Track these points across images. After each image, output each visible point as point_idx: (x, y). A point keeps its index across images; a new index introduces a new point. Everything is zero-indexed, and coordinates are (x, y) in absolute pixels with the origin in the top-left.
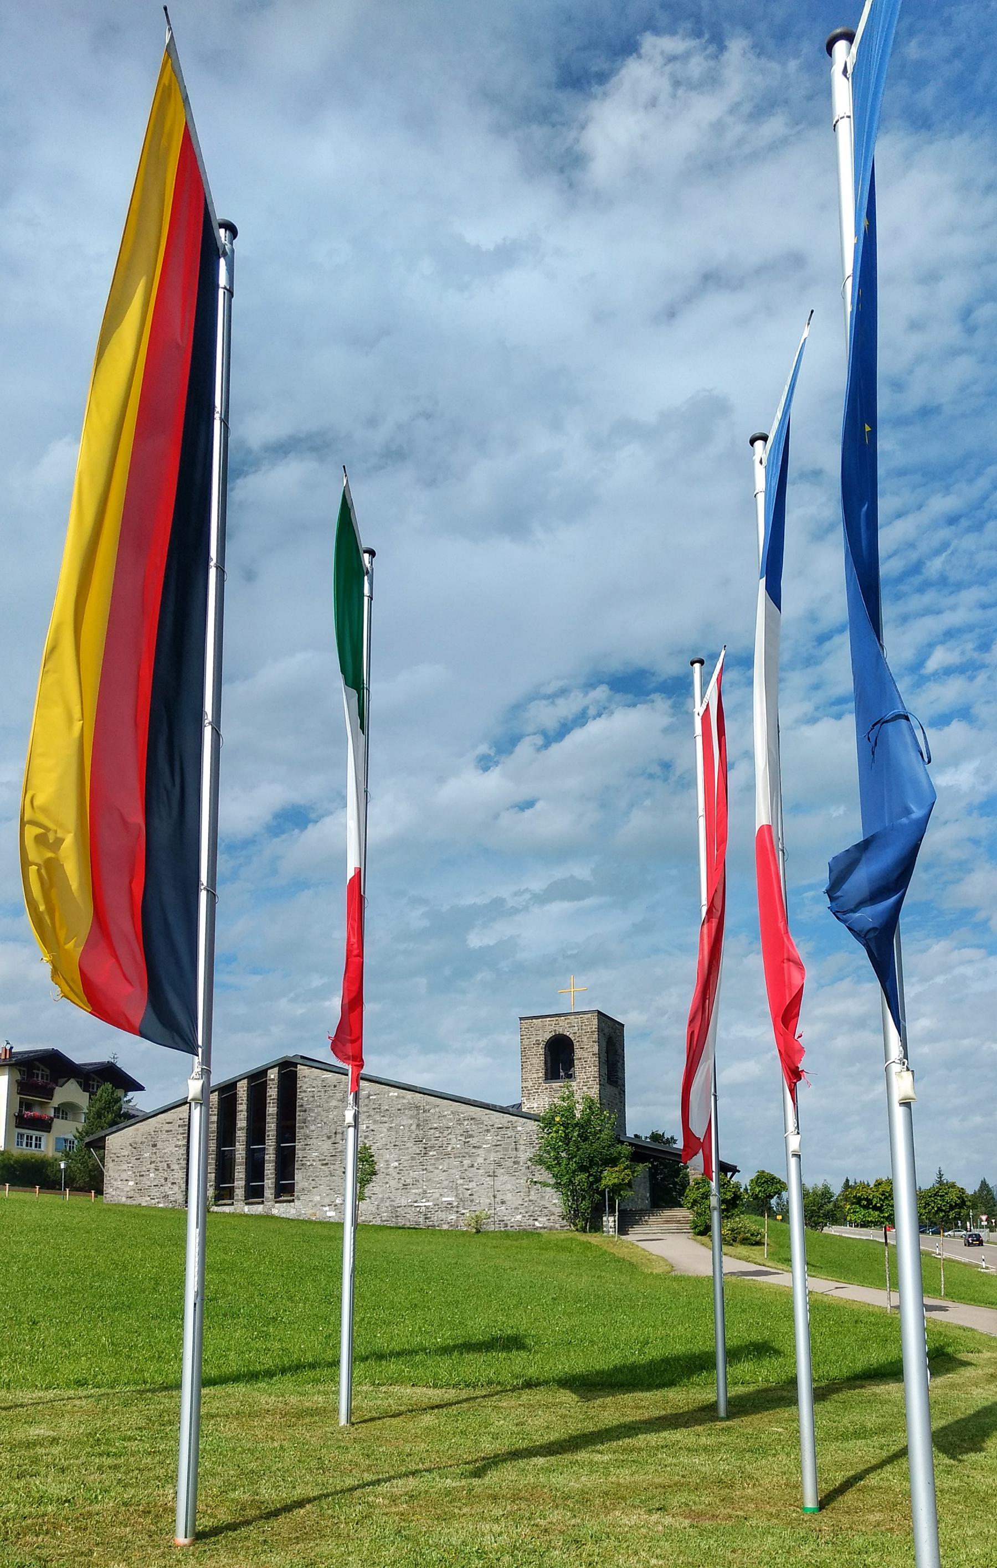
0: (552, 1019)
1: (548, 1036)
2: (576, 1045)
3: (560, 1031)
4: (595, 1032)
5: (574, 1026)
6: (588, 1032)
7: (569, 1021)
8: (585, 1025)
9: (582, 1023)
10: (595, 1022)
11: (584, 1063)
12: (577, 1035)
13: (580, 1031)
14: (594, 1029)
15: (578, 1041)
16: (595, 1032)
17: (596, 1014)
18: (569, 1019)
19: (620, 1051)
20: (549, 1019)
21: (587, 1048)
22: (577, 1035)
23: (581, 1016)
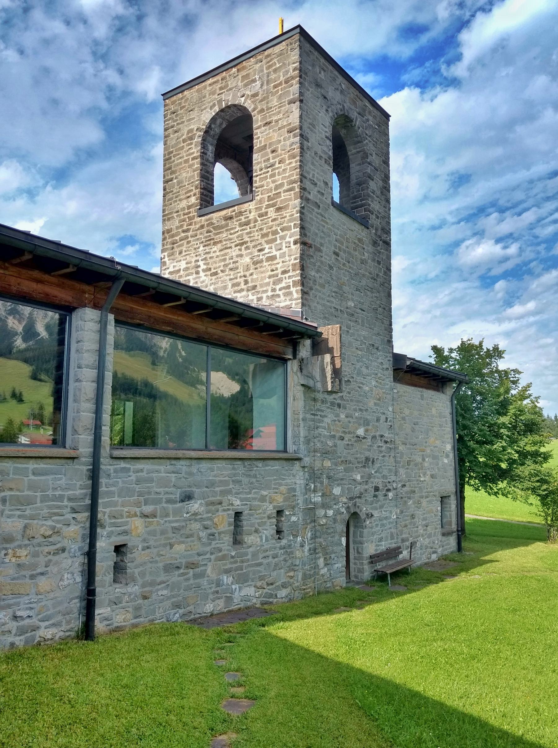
0: (215, 79)
1: (207, 116)
2: (257, 120)
3: (229, 99)
4: (293, 78)
5: (254, 81)
6: (280, 84)
7: (244, 73)
8: (275, 71)
9: (269, 67)
10: (295, 56)
11: (271, 156)
12: (260, 97)
13: (265, 87)
14: (291, 73)
15: (262, 110)
16: (293, 78)
17: (297, 37)
18: (244, 68)
19: (375, 160)
20: (211, 81)
21: (277, 121)
22: (260, 97)
23: (266, 53)
